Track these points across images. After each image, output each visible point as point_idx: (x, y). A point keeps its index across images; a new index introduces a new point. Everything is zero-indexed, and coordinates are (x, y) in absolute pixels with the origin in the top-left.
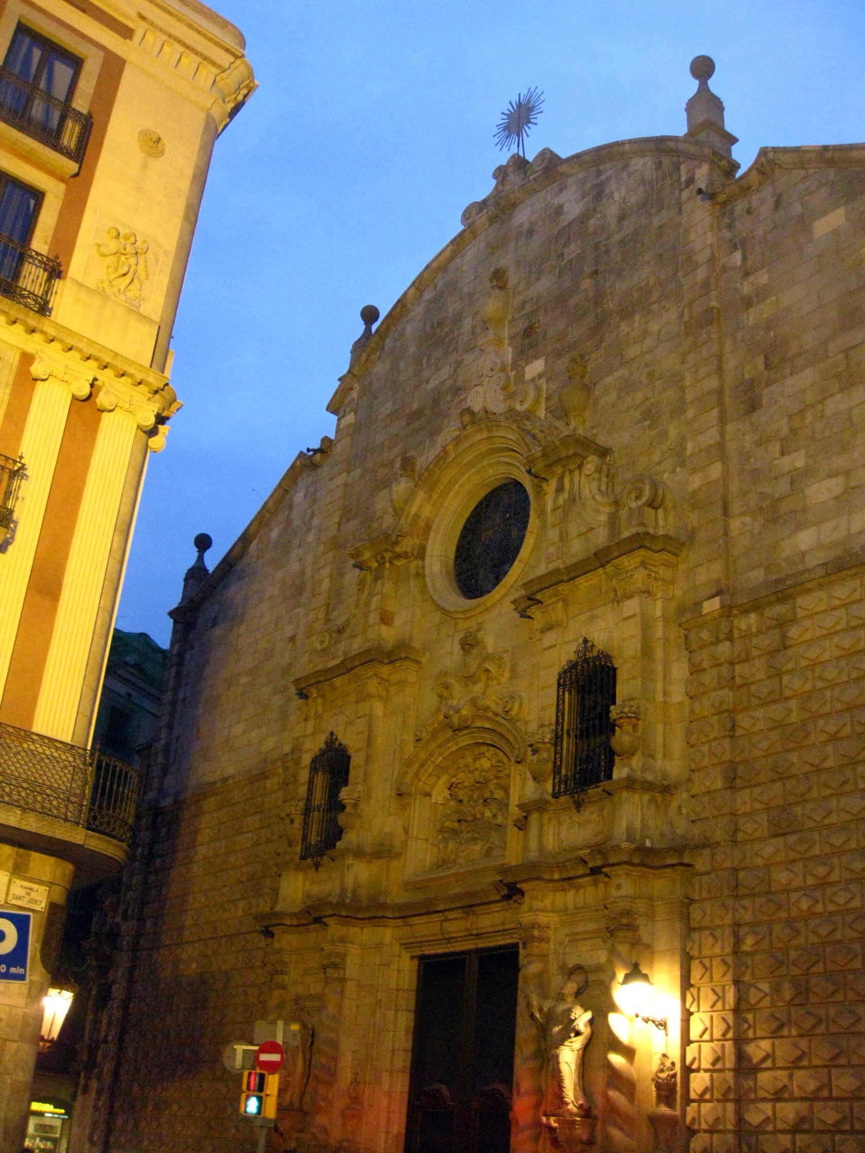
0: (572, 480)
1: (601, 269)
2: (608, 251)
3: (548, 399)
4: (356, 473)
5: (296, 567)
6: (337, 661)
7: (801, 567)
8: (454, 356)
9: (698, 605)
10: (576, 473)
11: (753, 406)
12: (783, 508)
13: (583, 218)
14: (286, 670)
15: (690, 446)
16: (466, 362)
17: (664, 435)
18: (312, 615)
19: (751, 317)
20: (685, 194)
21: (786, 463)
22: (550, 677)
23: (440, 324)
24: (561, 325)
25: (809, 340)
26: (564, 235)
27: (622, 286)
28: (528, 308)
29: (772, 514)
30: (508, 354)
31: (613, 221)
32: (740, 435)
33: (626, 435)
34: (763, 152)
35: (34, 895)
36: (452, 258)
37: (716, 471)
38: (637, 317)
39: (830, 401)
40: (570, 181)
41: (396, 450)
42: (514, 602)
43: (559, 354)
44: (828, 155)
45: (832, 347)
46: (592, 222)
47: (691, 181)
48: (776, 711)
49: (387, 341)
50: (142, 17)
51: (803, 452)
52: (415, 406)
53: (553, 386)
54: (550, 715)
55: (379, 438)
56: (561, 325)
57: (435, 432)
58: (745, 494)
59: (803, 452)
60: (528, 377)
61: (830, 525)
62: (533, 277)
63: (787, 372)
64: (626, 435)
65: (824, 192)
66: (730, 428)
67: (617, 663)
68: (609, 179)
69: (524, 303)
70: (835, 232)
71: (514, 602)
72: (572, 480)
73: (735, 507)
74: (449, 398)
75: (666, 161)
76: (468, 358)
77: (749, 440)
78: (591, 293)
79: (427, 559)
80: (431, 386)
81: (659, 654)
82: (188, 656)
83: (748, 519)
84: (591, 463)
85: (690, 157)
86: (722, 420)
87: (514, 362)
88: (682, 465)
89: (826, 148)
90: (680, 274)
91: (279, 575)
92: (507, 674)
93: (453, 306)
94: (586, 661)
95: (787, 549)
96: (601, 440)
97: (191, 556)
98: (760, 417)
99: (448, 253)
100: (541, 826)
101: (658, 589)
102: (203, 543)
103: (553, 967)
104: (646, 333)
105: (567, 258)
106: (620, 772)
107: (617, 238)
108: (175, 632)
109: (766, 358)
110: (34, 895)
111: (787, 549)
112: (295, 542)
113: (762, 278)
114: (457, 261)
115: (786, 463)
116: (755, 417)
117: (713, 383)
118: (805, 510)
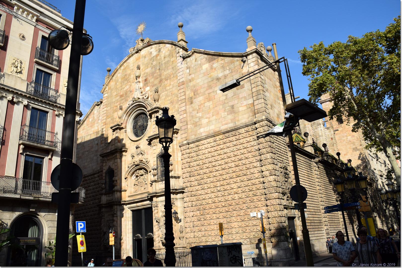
4: (109, 108)
5: (96, 128)
6: (109, 151)
7: (201, 136)
8: (129, 83)
9: (183, 142)
12: (198, 124)
13: (157, 56)
14: (97, 151)
17: (175, 107)
18: (102, 139)
19: (191, 84)
20: (178, 55)
21: (198, 115)
22: (155, 155)
25: (202, 90)
26: (152, 59)
27: (165, 73)
28: (145, 75)
29: (196, 125)
30: (141, 85)
31: (163, 58)
32: (189, 108)
37: (185, 115)
40: (153, 46)
41: (118, 103)
42: (147, 140)
43: (153, 87)
47: (179, 52)
53: (152, 93)
54: (156, 163)
55: (114, 100)
56: (153, 80)
57: (126, 100)
58: (191, 120)
65: (205, 59)
66: (188, 107)
69: (144, 73)
70: (207, 69)
71: (147, 140)
73: (189, 123)
75: (173, 46)
76: (133, 84)
77: (191, 109)
78: (159, 74)
81: (176, 151)
83: (191, 125)
86: (186, 105)
91: (93, 129)
93: (129, 72)
95: (198, 132)
104: (170, 84)
105: (153, 64)
107: (163, 62)
111: (198, 132)
112: (96, 122)
113: (193, 76)
114: (128, 61)
115: (198, 115)
116: (192, 105)
117: (184, 97)
118: (201, 124)
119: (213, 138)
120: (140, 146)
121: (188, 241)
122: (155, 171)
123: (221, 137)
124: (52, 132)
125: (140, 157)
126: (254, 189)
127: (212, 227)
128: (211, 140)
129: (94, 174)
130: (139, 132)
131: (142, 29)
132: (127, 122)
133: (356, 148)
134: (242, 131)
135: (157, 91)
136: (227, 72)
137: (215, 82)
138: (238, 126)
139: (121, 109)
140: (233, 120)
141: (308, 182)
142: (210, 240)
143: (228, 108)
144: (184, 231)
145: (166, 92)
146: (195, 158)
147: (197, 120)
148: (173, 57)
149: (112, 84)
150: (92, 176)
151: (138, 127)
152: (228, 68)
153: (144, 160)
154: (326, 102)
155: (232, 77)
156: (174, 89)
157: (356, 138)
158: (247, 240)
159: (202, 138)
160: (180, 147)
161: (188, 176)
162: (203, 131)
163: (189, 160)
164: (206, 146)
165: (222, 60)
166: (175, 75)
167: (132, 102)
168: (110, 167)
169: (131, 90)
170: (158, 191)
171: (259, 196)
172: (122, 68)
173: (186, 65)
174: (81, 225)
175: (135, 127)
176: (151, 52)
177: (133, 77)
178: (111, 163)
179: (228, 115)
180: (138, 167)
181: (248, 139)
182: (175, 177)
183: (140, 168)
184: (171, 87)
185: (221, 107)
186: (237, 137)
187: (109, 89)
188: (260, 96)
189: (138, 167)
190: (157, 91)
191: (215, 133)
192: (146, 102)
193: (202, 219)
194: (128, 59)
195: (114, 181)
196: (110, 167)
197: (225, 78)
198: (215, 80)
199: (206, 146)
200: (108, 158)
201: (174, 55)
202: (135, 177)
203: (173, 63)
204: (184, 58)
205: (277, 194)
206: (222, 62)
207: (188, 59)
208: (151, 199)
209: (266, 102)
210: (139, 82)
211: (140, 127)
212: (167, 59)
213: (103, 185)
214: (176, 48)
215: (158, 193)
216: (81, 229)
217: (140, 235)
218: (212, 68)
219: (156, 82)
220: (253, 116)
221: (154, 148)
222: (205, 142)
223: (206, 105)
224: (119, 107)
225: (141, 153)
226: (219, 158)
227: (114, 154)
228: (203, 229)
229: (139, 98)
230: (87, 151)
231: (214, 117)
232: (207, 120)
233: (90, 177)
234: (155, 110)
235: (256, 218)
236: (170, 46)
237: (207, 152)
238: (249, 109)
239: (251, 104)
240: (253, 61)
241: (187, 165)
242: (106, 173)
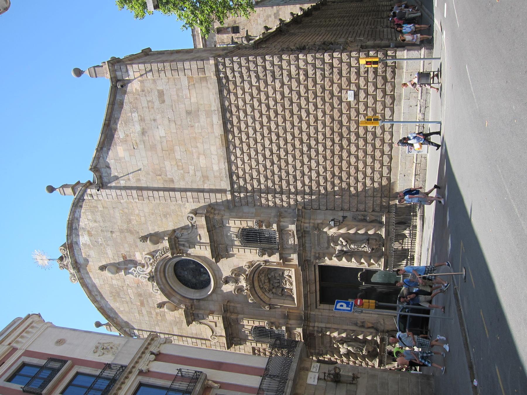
0: (181, 241)
1: (111, 230)
8: (125, 288)
10: (180, 239)
11: (172, 181)
16: (128, 283)
20: (95, 198)
21: (191, 172)
23: (111, 293)
24: (126, 245)
29: (205, 178)
31: (95, 224)
33: (170, 223)
34: (91, 169)
35: (315, 366)
36: (87, 288)
38: (132, 218)
39: (176, 157)
40: (74, 240)
43: (137, 246)
44: (99, 149)
45: (160, 155)
46: (92, 232)
47: (91, 195)
48: (262, 180)
49: (111, 316)
50: (10, 344)
51: (190, 167)
52: (139, 304)
55: (147, 318)
57: (150, 295)
59: (190, 167)
60: (141, 259)
61: (213, 160)
62: (105, 255)
63: (164, 169)
64: (170, 223)
70: (125, 150)
72: (181, 241)
74: (139, 290)
80: (133, 298)
83: (206, 185)
85: (83, 195)
86: (174, 190)
89: (97, 150)
90: (122, 201)
98: (176, 179)
99: (85, 289)
103: (326, 251)
104: (138, 215)
107: (102, 224)
109: (158, 176)
110: (315, 366)
115: (191, 172)
116: (175, 181)
118: (207, 167)
124: (175, 378)
132: (184, 297)
133: (275, 14)
135: (144, 239)
137: (147, 138)
138: (218, 108)
140: (209, 114)
143: (189, 120)
145: (149, 223)
147: (199, 174)
148: (97, 207)
155: (145, 109)
156: (146, 210)
157: (262, 12)
159: (227, 168)
166: (125, 205)
167: (155, 284)
169: (136, 285)
174: (342, 306)
179: (199, 122)
184: (142, 214)
185: (186, 132)
186: (234, 109)
190: (144, 239)
191: (222, 145)
197: (144, 120)
198: (144, 138)
201: (94, 205)
203: (106, 208)
212: (99, 218)
216: (347, 306)
218: (125, 141)
219: (130, 238)
223: (179, 157)
224: (158, 310)
231: (199, 145)
232: (202, 158)
238: (197, 85)
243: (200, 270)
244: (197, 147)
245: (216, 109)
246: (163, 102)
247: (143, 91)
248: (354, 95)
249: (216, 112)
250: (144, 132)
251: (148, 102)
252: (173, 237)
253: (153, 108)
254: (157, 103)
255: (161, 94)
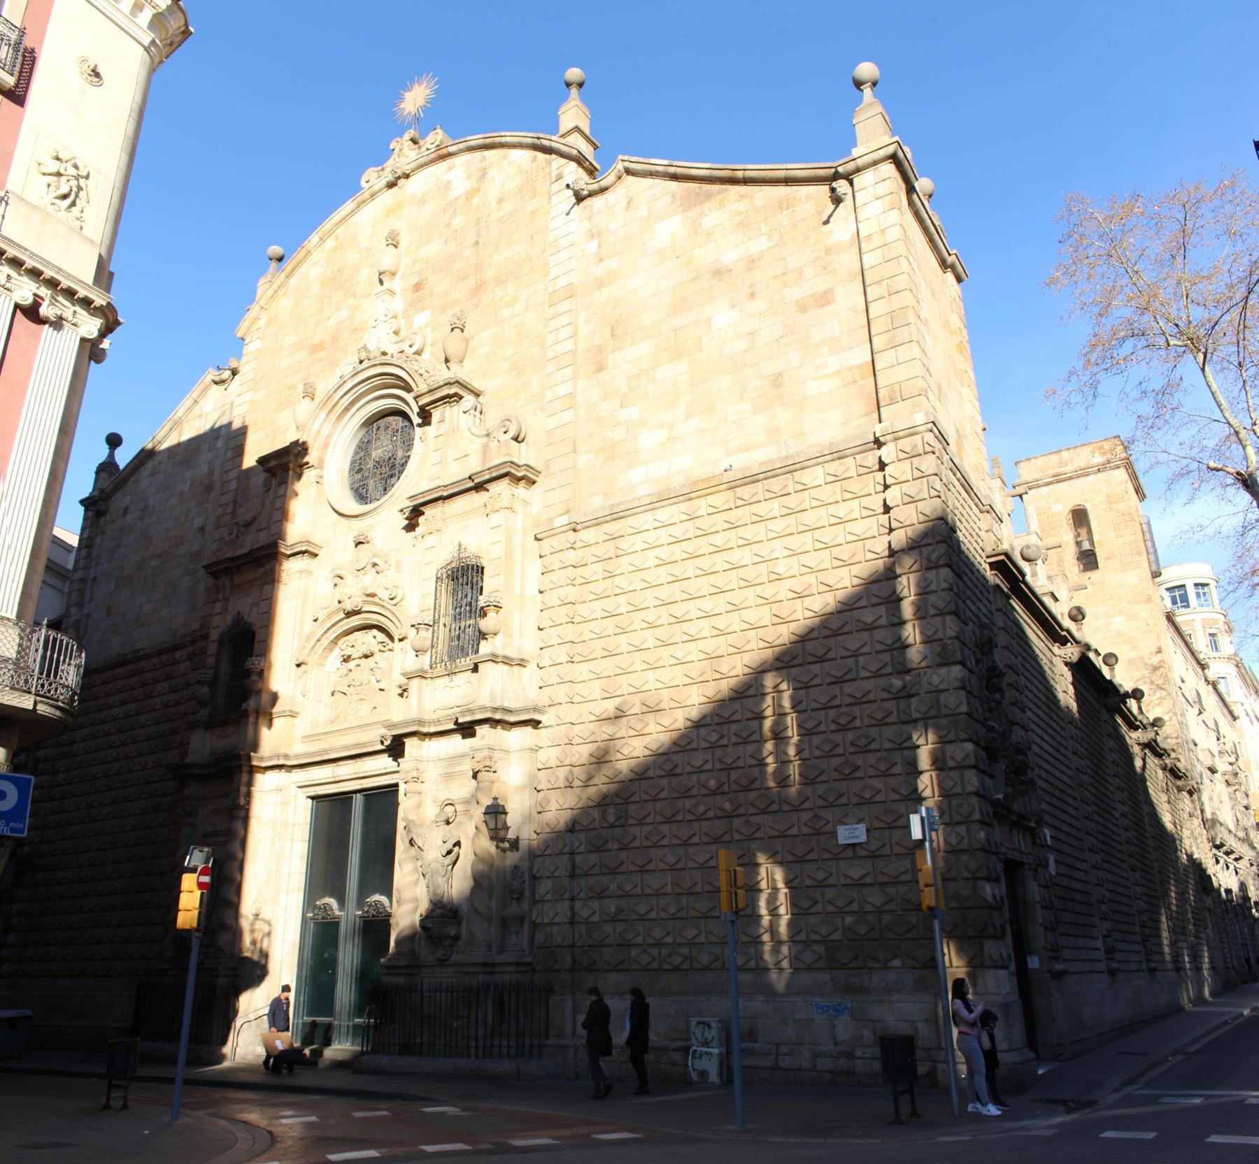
2: (488, 227)
3: (432, 345)
5: (204, 469)
6: (244, 551)
9: (550, 520)
11: (600, 368)
13: (469, 195)
15: (549, 395)
18: (220, 510)
20: (556, 187)
30: (398, 304)
37: (569, 416)
43: (444, 309)
48: (608, 604)
52: (316, 340)
57: (334, 364)
65: (668, 199)
67: (484, 563)
68: (491, 165)
79: (326, 469)
80: (331, 323)
82: (98, 540)
84: (469, 400)
87: (405, 315)
88: (542, 409)
90: (547, 253)
92: (392, 569)
94: (460, 559)
96: (476, 384)
97: (102, 453)
100: (420, 689)
101: (519, 508)
102: (114, 441)
106: (485, 647)
108: (85, 519)
117: (568, 346)
119: (683, 506)
120: (370, 535)
121: (540, 937)
122: (423, 633)
123: (719, 500)
125: (369, 581)
126: (858, 723)
127: (654, 882)
128: (673, 512)
129: (173, 648)
130: (371, 483)
131: (421, 102)
132: (326, 445)
134: (814, 476)
136: (760, 244)
139: (309, 394)
141: (1051, 731)
142: (639, 940)
144: (527, 894)
146: (598, 588)
149: (284, 304)
150: (165, 657)
151: (371, 465)
152: (764, 229)
153: (383, 595)
154: (1039, 486)
158: (817, 948)
159: (636, 504)
160: (537, 539)
161: (564, 659)
162: (640, 480)
163: (572, 593)
164: (651, 537)
165: (743, 197)
168: (239, 619)
170: (426, 717)
171: (884, 754)
172: (330, 243)
173: (586, 225)
175: (357, 467)
176: (449, 183)
177: (367, 275)
178: (248, 600)
180: (355, 621)
181: (842, 510)
182: (507, 661)
183: (363, 622)
186: (792, 502)
187: (269, 323)
188: (903, 334)
189: (355, 621)
192: (413, 366)
193: (610, 846)
194: (352, 212)
195: (248, 673)
196: (239, 619)
197: (750, 269)
199: (651, 537)
200: (238, 580)
202: (338, 663)
204: (580, 198)
205: (970, 746)
206: (743, 206)
207: (597, 201)
208: (396, 749)
209: (925, 360)
210: (392, 293)
211: (378, 464)
213: (205, 690)
214: (549, 163)
215: (430, 723)
217: (332, 902)
220: (868, 414)
221: (430, 541)
222: (647, 520)
224: (301, 388)
225: (375, 565)
226: (703, 585)
227: (263, 565)
228: (613, 887)
229: (384, 354)
230: (160, 556)
233: (156, 660)
234: (445, 391)
235: (861, 852)
236: (527, 154)
237: (652, 562)
239: (859, 367)
240: (880, 192)
241: (561, 614)
242: (221, 642)
243: (392, 476)
244: (688, 417)
245: (791, 452)
246: (803, 309)
247: (828, 251)
248: (854, 845)
249: (784, 454)
250: (719, 273)
251: (800, 270)
252: (461, 392)
253: (785, 285)
254: (796, 293)
255: (825, 299)
